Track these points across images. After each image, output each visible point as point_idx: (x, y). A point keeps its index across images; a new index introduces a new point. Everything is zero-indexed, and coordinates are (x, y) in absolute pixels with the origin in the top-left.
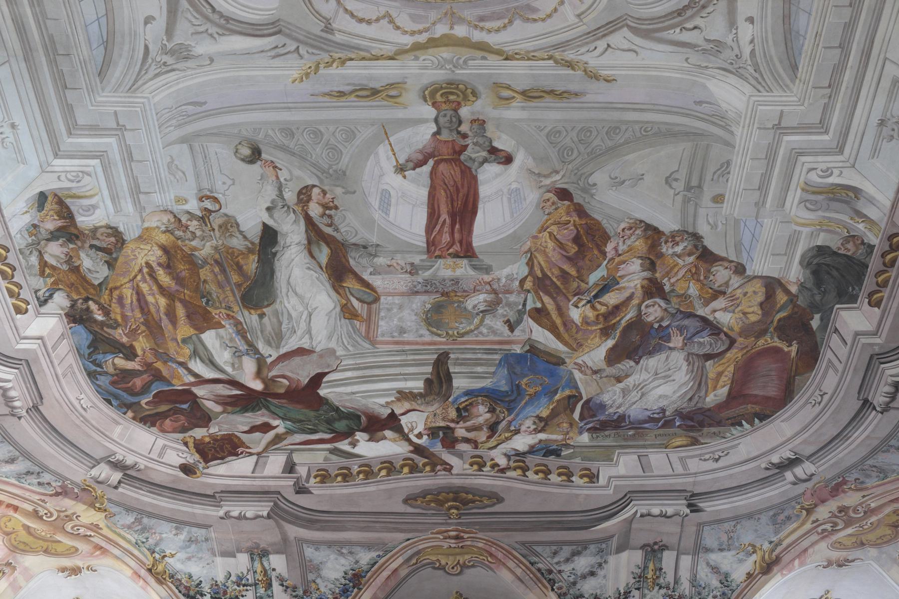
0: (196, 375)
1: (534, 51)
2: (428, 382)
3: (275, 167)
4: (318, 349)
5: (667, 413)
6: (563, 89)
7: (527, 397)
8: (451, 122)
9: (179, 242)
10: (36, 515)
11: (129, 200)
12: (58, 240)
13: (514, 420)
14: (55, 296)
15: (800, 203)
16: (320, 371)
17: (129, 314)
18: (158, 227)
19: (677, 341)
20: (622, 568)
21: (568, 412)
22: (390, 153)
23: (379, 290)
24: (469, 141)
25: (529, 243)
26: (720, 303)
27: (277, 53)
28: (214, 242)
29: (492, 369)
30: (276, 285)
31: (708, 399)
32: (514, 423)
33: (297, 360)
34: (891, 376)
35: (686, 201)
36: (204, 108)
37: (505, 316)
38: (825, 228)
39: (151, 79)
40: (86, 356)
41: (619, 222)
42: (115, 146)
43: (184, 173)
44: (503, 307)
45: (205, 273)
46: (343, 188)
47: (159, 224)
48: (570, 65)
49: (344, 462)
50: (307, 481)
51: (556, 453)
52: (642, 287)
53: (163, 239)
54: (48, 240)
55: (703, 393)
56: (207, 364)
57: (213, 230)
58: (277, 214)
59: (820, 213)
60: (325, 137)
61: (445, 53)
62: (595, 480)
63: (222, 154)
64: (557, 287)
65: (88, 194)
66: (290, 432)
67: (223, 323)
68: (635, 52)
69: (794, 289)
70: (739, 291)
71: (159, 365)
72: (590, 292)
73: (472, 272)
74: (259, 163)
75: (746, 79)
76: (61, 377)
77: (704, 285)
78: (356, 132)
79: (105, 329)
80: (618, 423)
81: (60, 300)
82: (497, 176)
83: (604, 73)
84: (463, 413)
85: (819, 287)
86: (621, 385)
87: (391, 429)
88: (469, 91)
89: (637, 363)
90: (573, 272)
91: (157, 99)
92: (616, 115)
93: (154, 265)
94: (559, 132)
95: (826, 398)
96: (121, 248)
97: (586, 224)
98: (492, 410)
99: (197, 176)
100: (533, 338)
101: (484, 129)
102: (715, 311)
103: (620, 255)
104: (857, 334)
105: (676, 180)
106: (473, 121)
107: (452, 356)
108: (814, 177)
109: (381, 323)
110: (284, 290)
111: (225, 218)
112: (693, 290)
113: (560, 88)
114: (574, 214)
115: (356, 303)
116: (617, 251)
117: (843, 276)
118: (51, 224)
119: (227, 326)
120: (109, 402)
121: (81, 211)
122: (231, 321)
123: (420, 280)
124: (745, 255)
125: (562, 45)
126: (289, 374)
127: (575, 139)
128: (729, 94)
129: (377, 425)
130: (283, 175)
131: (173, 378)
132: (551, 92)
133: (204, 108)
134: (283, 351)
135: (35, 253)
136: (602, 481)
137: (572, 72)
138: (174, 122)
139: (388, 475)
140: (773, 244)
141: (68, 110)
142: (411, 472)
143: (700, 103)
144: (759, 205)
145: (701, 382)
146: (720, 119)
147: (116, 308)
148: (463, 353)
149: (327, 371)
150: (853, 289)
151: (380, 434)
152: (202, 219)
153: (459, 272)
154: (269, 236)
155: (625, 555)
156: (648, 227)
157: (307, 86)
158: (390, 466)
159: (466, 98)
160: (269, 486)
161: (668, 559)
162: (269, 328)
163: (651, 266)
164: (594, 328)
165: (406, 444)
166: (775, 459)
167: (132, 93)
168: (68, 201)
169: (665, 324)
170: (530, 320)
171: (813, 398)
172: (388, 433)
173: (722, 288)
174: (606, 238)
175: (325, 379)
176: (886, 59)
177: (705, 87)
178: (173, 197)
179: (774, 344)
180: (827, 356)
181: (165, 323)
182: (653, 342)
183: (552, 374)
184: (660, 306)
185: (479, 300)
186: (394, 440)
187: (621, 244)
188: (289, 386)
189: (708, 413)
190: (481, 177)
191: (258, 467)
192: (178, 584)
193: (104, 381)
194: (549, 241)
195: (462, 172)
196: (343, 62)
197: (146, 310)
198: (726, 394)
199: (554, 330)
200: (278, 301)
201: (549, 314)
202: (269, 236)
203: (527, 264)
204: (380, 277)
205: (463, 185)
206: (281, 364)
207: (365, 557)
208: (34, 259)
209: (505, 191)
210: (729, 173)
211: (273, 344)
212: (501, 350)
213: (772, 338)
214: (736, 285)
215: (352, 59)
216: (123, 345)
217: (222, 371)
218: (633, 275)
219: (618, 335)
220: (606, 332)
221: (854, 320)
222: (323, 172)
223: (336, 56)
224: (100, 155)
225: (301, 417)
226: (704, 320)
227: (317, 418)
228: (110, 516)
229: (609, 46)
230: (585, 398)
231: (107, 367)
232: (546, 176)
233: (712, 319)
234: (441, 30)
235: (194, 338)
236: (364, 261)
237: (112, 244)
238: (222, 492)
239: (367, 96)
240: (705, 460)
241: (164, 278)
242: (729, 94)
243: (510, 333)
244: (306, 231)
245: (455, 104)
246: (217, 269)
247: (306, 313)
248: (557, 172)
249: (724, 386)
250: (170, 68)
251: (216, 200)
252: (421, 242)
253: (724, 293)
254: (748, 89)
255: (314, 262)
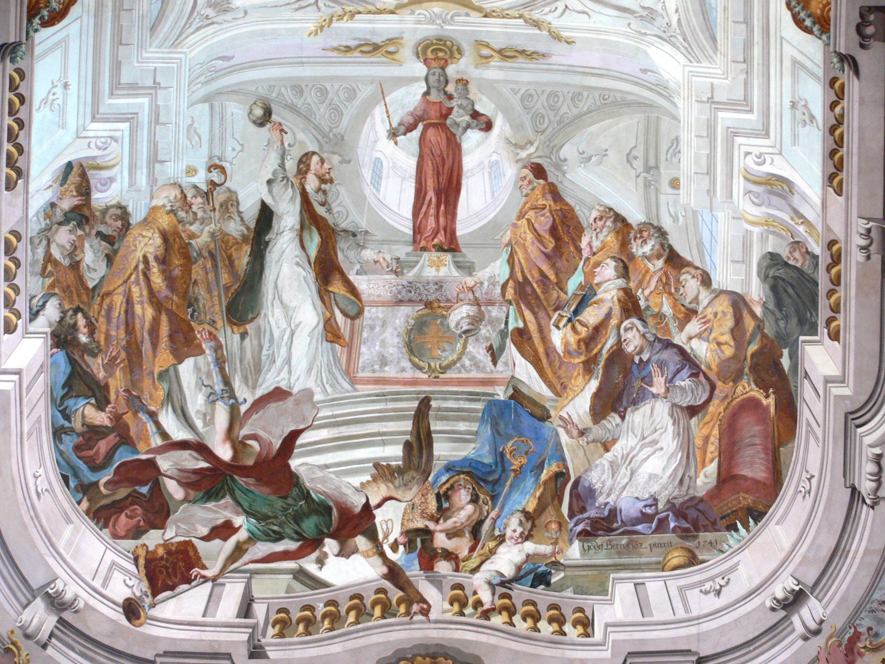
0: (164, 435)
1: (508, 9)
2: (408, 446)
3: (282, 130)
4: (295, 391)
5: (660, 506)
6: (532, 49)
7: (513, 475)
8: (439, 81)
9: (180, 227)
11: (145, 171)
12: (69, 223)
13: (498, 516)
14: (48, 305)
15: (745, 194)
16: (293, 429)
17: (113, 333)
18: (164, 206)
19: (658, 385)
21: (556, 502)
22: (385, 115)
23: (364, 297)
24: (454, 103)
25: (509, 233)
26: (693, 327)
28: (213, 226)
29: (474, 427)
30: (264, 289)
31: (699, 482)
32: (498, 522)
33: (272, 408)
34: (871, 446)
35: (647, 185)
36: (232, 62)
37: (487, 339)
38: (771, 229)
39: (193, 33)
40: (58, 402)
41: (592, 208)
42: (147, 106)
43: (200, 138)
44: (485, 326)
45: (197, 272)
46: (340, 155)
47: (165, 201)
48: (537, 24)
50: (264, 635)
52: (619, 300)
53: (165, 221)
54: (60, 224)
55: (692, 472)
56: (177, 416)
57: (214, 209)
58: (277, 188)
59: (763, 209)
60: (330, 95)
62: (589, 630)
63: (237, 112)
64: (538, 298)
65: (110, 164)
66: (252, 539)
67: (204, 346)
68: (588, 14)
69: (758, 311)
70: (709, 310)
71: (128, 418)
72: (569, 307)
73: (455, 273)
74: (268, 125)
75: (678, 48)
76: (25, 436)
77: (676, 300)
78: (358, 91)
79: (86, 357)
81: (52, 312)
82: (479, 144)
83: (564, 34)
85: (781, 310)
86: (609, 456)
87: (363, 534)
88: (455, 48)
89: (623, 418)
90: (552, 277)
91: (193, 54)
92: (577, 80)
93: (151, 258)
94: (531, 96)
95: (814, 481)
96: (124, 236)
97: (561, 210)
98: (474, 500)
99: (211, 140)
100: (517, 376)
101: (467, 90)
102: (690, 338)
103: (594, 254)
104: (827, 380)
105: (636, 158)
106: (459, 81)
107: (433, 404)
108: (750, 162)
109: (364, 349)
110: (270, 297)
111: (228, 194)
112: (667, 309)
113: (530, 48)
114: (549, 196)
115: (339, 317)
116: (591, 247)
117: (798, 295)
118: (66, 204)
119: (208, 352)
120: (65, 479)
121: (99, 186)
122: (212, 344)
123: (405, 283)
124: (707, 258)
126: (261, 433)
127: (546, 104)
128: (668, 63)
129: (351, 524)
130: (288, 139)
131: (140, 439)
132: (523, 52)
133: (232, 62)
134: (260, 392)
135: (44, 242)
137: (538, 32)
138: (202, 79)
139: (357, 622)
141: (117, 66)
142: (383, 617)
143: (645, 71)
144: (711, 192)
146: (662, 88)
147: (102, 325)
148: (445, 399)
149: (301, 427)
150: (811, 314)
151: (351, 542)
152: (207, 196)
153: (443, 272)
154: (266, 216)
156: (619, 219)
157: (320, 40)
159: (452, 56)
160: (219, 643)
162: (249, 355)
163: (624, 271)
164: (577, 361)
165: (377, 560)
167: (174, 48)
168: (90, 173)
169: (645, 357)
170: (513, 347)
171: (802, 484)
172: (361, 541)
173: (693, 305)
175: (300, 441)
176: (782, 38)
177: (646, 54)
178: (184, 168)
179: (752, 393)
180: (804, 415)
181: (147, 346)
182: (637, 384)
183: (538, 437)
184: (638, 329)
185: (459, 315)
186: (366, 555)
187: (594, 238)
188: (260, 454)
189: (701, 507)
190: (465, 146)
191: (211, 604)
193: (69, 442)
194: (528, 231)
195: (448, 139)
196: (352, 15)
197: (130, 328)
198: (715, 475)
200: (262, 314)
201: (530, 338)
202: (266, 216)
203: (508, 261)
204: (365, 277)
205: (448, 156)
206: (255, 416)
208: (41, 251)
209: (486, 163)
210: (679, 152)
211: (250, 383)
212: (484, 394)
213: (749, 385)
214: (706, 302)
215: (360, 13)
216: (97, 383)
217: (191, 426)
219: (601, 371)
220: (588, 367)
222: (324, 136)
223: (348, 9)
224: (130, 118)
225: (265, 510)
226: (681, 351)
227: (285, 510)
229: (566, 7)
230: (573, 479)
231: (75, 421)
232: (522, 148)
233: (689, 351)
235: (172, 372)
236: (352, 254)
237: (115, 230)
238: (166, 654)
239: (369, 52)
240: (706, 593)
241: (157, 280)
242: (668, 63)
243: (492, 367)
244: (301, 211)
245: (442, 62)
246: (209, 265)
247: (288, 331)
248: (532, 143)
249: (712, 461)
250: (210, 21)
251: (223, 170)
252: (407, 228)
253: (695, 312)
255: (304, 255)
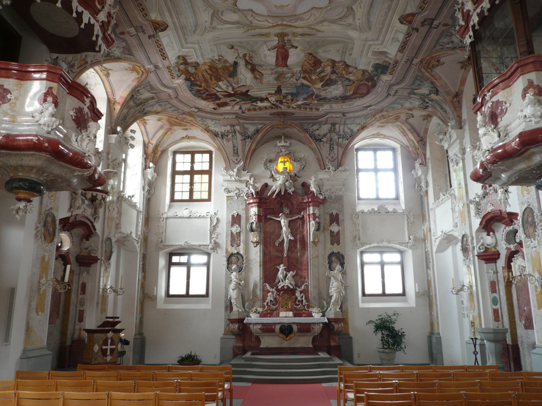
2: (276, 91)
10: (177, 118)
19: (340, 82)
20: (325, 129)
26: (351, 75)
27: (238, 28)
33: (243, 87)
48: (313, 29)
49: (254, 107)
51: (309, 105)
53: (209, 64)
61: (281, 27)
66: (240, 101)
80: (325, 99)
81: (183, 76)
84: (285, 97)
99: (218, 52)
108: (375, 50)
112: (344, 72)
113: (310, 33)
118: (181, 62)
125: (311, 25)
128: (353, 34)
132: (308, 34)
136: (320, 110)
140: (364, 62)
141: (186, 39)
144: (361, 55)
145: (346, 90)
146: (351, 39)
154: (236, 64)
155: (326, 126)
156: (332, 60)
158: (266, 108)
161: (337, 126)
166: (365, 105)
174: (321, 62)
180: (378, 85)
181: (209, 80)
185: (289, 75)
192: (213, 133)
193: (194, 92)
196: (255, 29)
199: (308, 81)
202: (236, 64)
207: (259, 126)
208: (177, 69)
218: (329, 70)
220: (321, 81)
221: (386, 78)
226: (347, 78)
228: (195, 118)
234: (279, 23)
237: (196, 65)
241: (209, 71)
242: (353, 34)
252: (274, 64)
254: (358, 33)
